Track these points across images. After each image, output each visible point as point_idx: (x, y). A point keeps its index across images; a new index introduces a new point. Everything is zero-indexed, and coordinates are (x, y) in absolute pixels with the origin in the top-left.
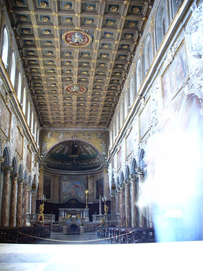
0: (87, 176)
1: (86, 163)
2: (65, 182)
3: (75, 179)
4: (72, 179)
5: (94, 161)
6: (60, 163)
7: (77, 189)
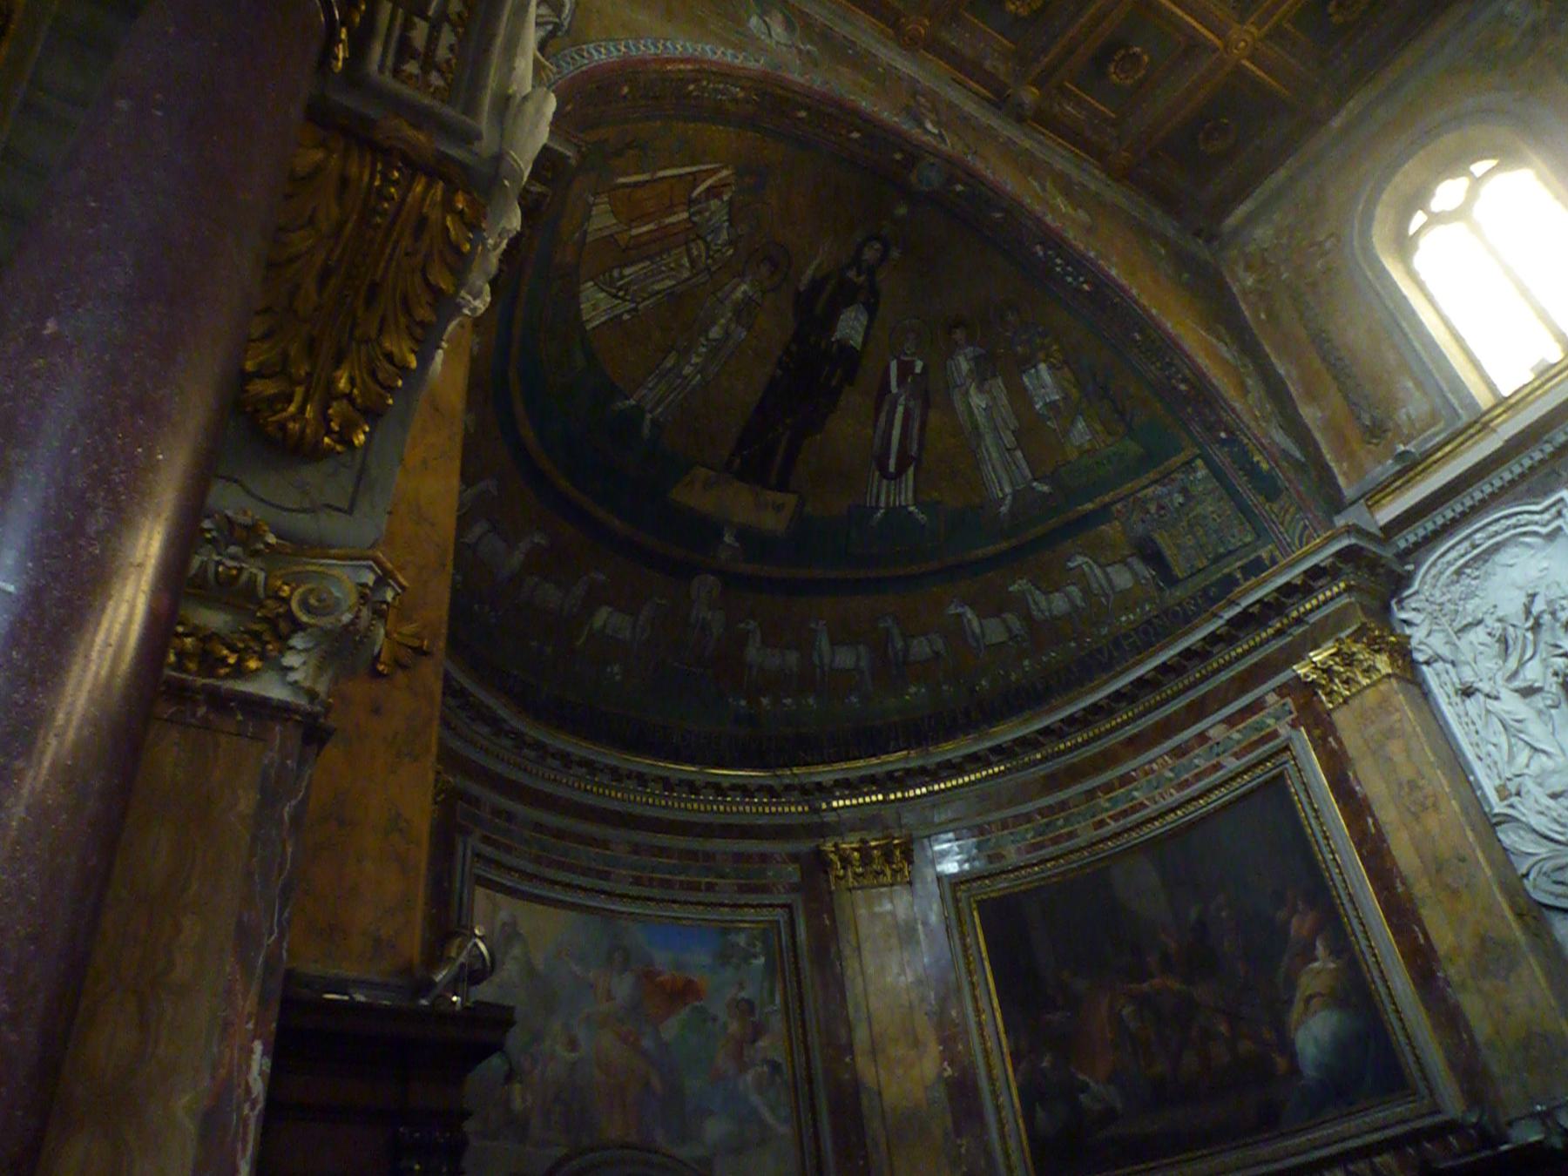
0: (805, 846)
1: (845, 658)
2: (507, 909)
3: (637, 881)
4: (604, 876)
5: (994, 606)
6: (517, 559)
7: (671, 1028)
